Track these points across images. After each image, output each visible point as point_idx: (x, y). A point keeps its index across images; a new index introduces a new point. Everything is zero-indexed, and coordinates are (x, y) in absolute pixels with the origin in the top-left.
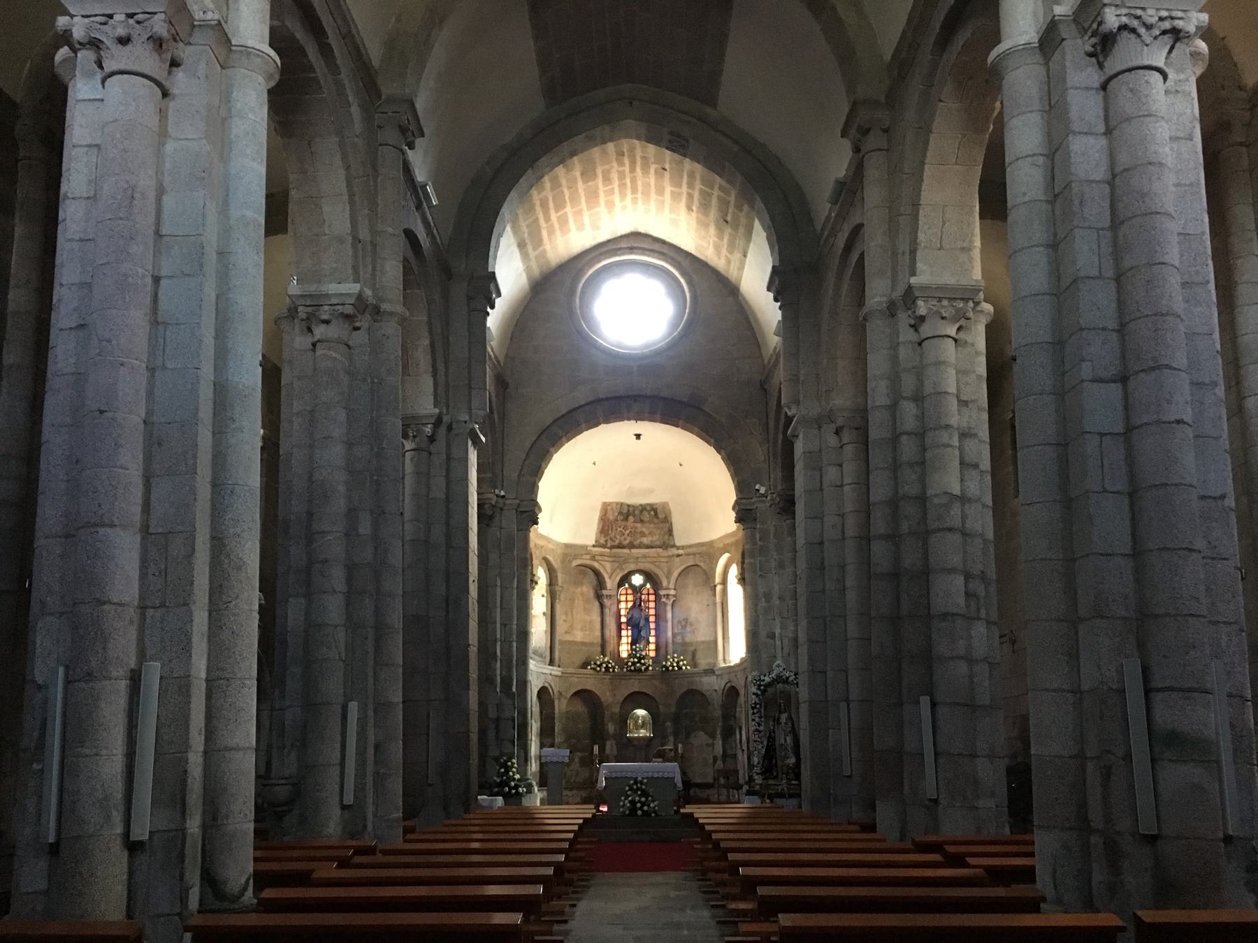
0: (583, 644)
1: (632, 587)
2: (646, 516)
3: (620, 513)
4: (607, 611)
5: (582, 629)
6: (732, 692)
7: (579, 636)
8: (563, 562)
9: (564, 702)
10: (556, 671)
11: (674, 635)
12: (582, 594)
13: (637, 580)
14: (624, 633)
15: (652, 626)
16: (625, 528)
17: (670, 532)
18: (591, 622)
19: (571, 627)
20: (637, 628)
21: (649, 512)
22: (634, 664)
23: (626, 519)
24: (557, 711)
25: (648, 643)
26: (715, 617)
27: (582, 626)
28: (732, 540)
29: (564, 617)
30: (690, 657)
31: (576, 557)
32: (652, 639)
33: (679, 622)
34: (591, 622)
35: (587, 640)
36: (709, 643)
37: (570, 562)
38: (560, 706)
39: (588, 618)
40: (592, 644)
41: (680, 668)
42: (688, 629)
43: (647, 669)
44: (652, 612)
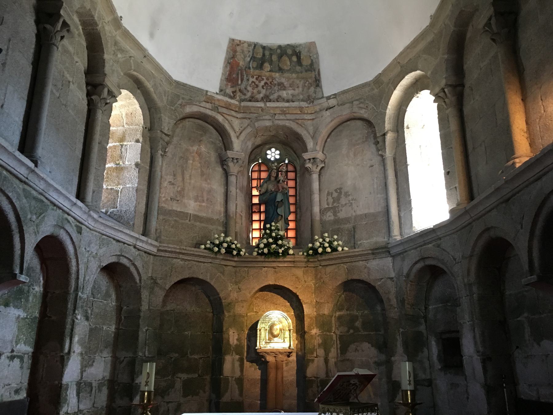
0: (197, 218)
1: (267, 162)
2: (286, 63)
3: (253, 58)
4: (233, 179)
5: (196, 199)
6: (432, 273)
7: (191, 206)
8: (172, 103)
9: (161, 294)
10: (148, 244)
11: (322, 212)
12: (199, 154)
13: (273, 154)
14: (256, 217)
15: (292, 200)
16: (259, 78)
17: (317, 82)
18: (210, 191)
19: (181, 193)
20: (272, 207)
21: (290, 57)
22: (267, 245)
23: (260, 66)
24: (145, 307)
25: (287, 222)
26: (385, 178)
27: (199, 193)
28: (421, 46)
29: (170, 178)
30: (345, 238)
31: (190, 102)
32: (291, 217)
33: (328, 194)
34: (210, 191)
35: (204, 215)
36: (374, 215)
37: (182, 106)
38: (150, 301)
39: (205, 185)
40: (209, 220)
41: (334, 250)
42: (343, 201)
43: (286, 253)
44: (292, 192)
